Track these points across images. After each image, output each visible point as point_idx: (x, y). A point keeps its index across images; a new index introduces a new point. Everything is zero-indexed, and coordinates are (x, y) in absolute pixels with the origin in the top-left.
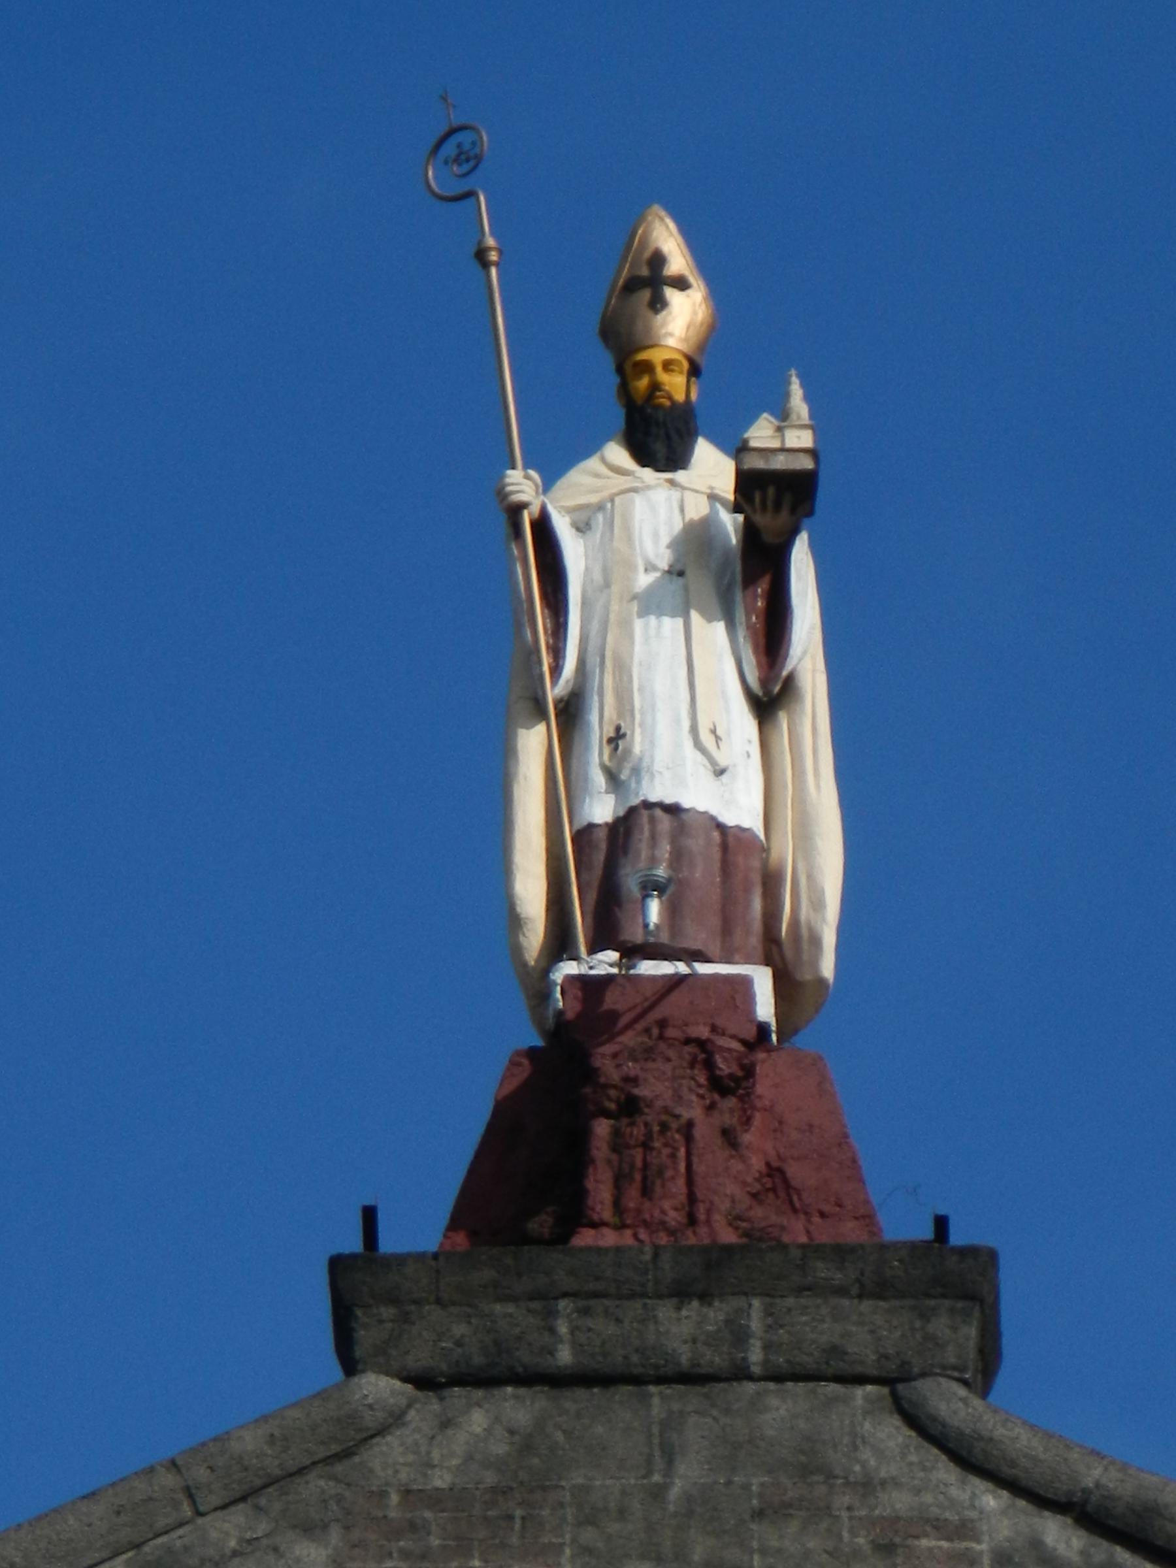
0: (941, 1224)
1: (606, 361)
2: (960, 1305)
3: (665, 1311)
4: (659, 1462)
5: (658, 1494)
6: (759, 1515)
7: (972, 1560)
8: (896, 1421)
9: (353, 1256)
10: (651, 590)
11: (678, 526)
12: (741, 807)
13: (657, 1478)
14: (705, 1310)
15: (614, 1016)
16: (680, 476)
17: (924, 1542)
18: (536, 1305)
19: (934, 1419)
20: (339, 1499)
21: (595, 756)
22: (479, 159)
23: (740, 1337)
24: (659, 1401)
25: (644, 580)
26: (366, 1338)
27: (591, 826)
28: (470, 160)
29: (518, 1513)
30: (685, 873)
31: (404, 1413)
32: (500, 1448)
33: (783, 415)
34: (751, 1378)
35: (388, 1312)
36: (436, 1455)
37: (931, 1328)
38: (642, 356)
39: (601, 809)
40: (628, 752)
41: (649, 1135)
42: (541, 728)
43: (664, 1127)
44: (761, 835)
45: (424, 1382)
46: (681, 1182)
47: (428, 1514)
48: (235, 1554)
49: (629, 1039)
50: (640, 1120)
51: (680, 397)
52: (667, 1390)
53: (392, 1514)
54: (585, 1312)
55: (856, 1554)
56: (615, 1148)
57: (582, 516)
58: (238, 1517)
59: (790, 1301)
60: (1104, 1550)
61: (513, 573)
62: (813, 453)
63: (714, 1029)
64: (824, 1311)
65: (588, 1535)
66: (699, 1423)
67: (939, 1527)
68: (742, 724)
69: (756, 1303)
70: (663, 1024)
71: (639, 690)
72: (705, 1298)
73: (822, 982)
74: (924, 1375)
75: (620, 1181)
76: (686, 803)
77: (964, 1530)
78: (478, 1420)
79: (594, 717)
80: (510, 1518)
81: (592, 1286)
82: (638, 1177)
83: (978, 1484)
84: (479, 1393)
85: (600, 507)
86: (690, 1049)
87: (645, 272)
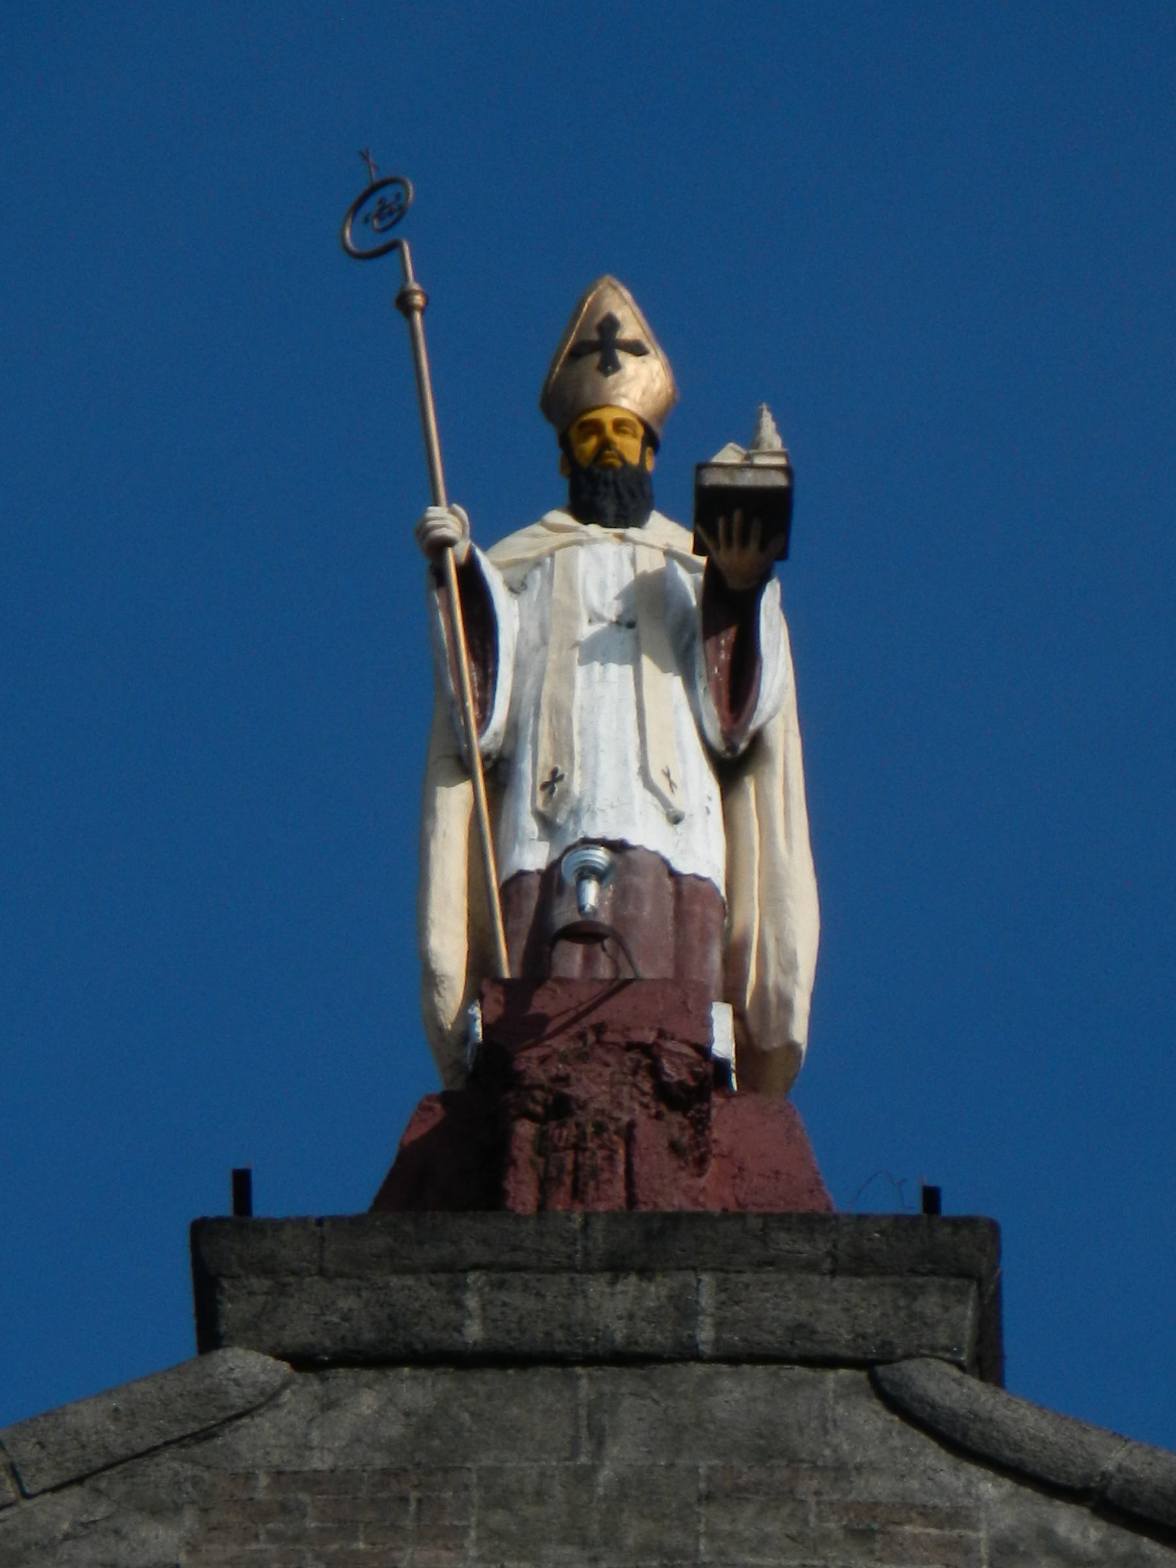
0: (931, 1197)
1: (549, 434)
2: (953, 1282)
3: (596, 1286)
4: (586, 1446)
5: (584, 1476)
6: (708, 1498)
7: (967, 1549)
8: (876, 1405)
9: (221, 1220)
10: (595, 639)
11: (629, 577)
12: (700, 853)
13: (583, 1460)
14: (644, 1284)
15: (543, 1020)
16: (632, 532)
17: (908, 1528)
18: (442, 1278)
19: (921, 1400)
20: (196, 1481)
21: (526, 801)
22: (402, 210)
23: (686, 1312)
24: (586, 1382)
25: (586, 631)
26: (233, 1310)
27: (522, 874)
28: (393, 214)
29: (414, 1495)
30: (631, 910)
31: (277, 1394)
32: (394, 1430)
33: (751, 440)
34: (699, 1358)
35: (260, 1284)
36: (315, 1436)
37: (917, 1306)
38: (593, 416)
39: (533, 856)
40: (566, 792)
41: (582, 1136)
42: (465, 788)
43: (600, 1128)
44: (720, 882)
45: (304, 1361)
46: (619, 1187)
47: (304, 1497)
48: (67, 1537)
49: (560, 1044)
50: (571, 1122)
51: (633, 458)
52: (597, 1372)
53: (261, 1495)
54: (501, 1285)
55: (825, 1538)
56: (540, 1152)
57: (518, 574)
58: (73, 1498)
59: (746, 1277)
60: (1125, 1542)
61: (434, 624)
62: (787, 470)
63: (661, 1034)
64: (789, 1287)
65: (498, 1518)
66: (634, 1406)
67: (926, 1514)
68: (700, 785)
69: (706, 1278)
70: (600, 1029)
71: (580, 733)
72: (645, 1272)
73: (792, 1047)
74: (908, 1356)
75: (545, 1185)
76: (633, 840)
77: (956, 1517)
78: (367, 1402)
79: (526, 766)
80: (404, 1500)
81: (506, 1258)
82: (568, 1180)
83: (972, 1469)
84: (369, 1375)
85: (538, 563)
86: (633, 1055)
87: (594, 336)
